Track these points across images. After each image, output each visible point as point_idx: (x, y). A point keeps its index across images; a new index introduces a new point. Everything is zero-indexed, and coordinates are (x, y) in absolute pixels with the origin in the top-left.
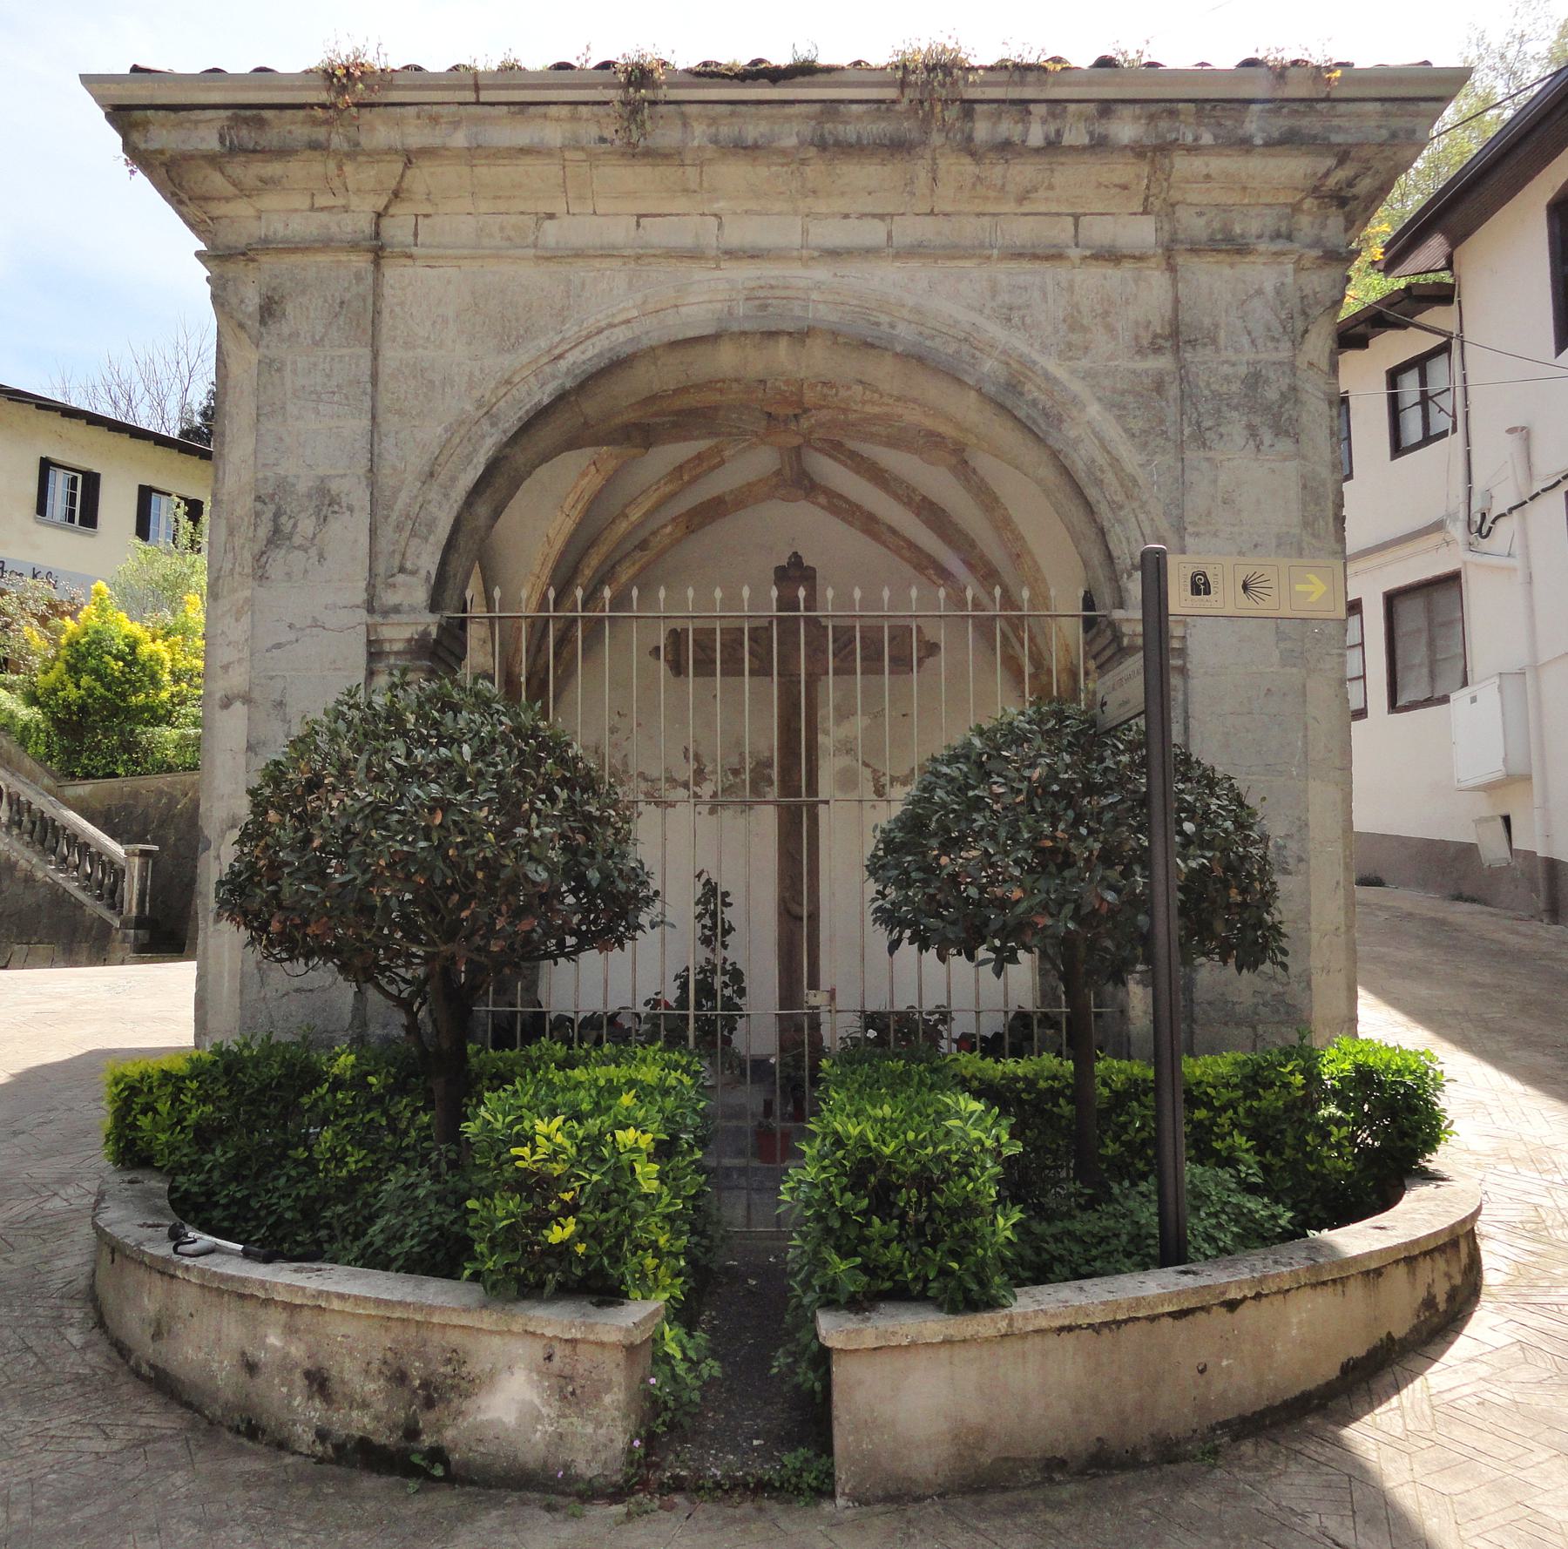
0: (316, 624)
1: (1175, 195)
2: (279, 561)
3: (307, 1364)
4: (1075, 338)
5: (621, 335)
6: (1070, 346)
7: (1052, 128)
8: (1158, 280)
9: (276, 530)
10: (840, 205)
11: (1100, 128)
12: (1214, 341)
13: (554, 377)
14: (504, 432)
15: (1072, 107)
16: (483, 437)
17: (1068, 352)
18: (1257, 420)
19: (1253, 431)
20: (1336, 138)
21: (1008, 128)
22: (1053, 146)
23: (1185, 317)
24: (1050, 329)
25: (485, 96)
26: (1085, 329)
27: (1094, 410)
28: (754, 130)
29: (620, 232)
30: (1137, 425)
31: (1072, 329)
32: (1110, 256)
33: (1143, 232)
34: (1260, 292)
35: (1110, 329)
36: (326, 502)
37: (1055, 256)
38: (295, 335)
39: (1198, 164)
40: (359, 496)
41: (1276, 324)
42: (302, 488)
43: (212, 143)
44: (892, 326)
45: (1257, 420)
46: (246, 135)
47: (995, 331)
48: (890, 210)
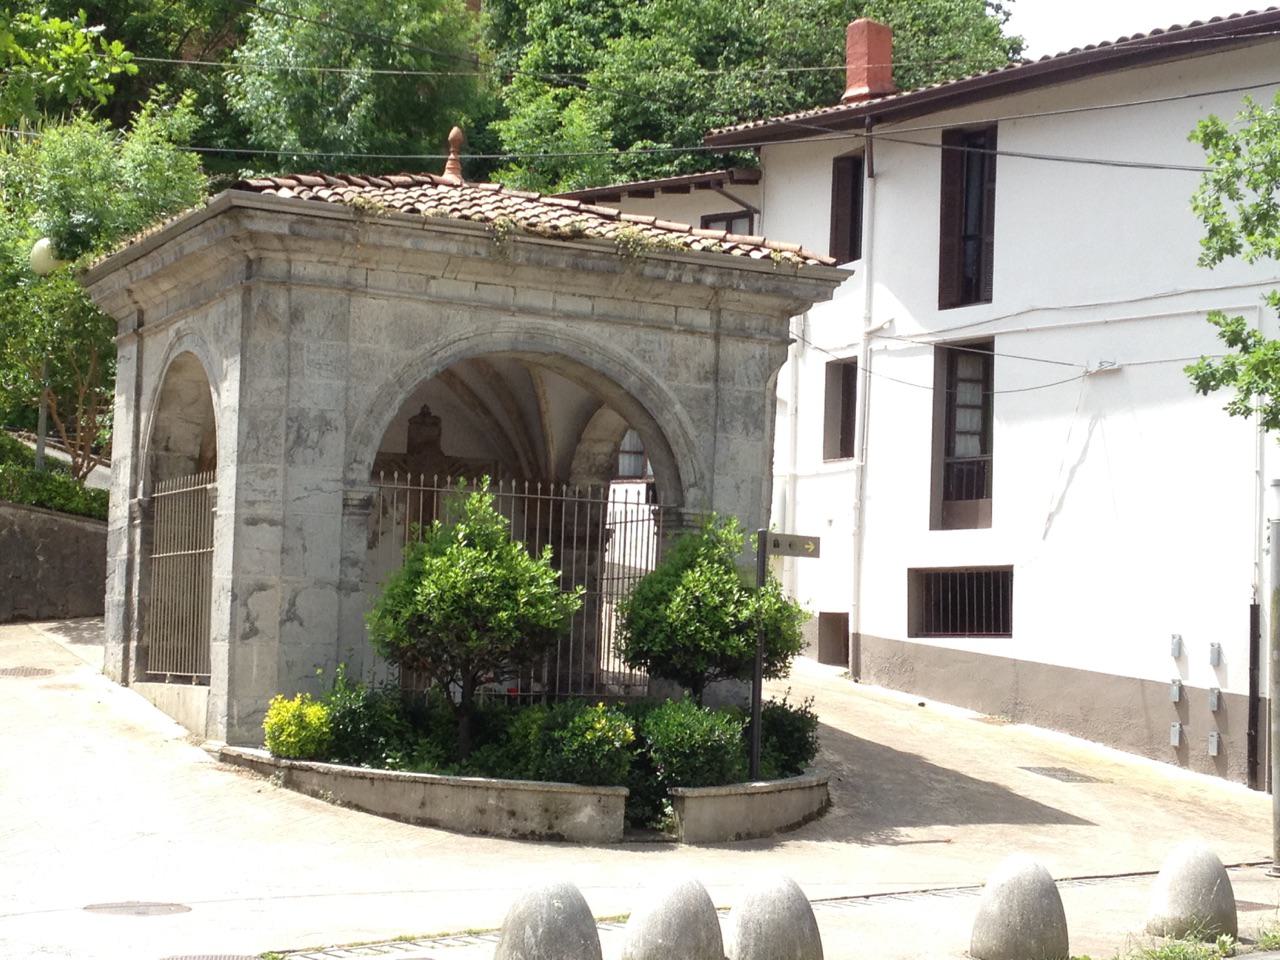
0: (319, 489)
1: (722, 306)
2: (300, 454)
3: (507, 808)
4: (673, 370)
5: (464, 344)
6: (670, 373)
7: (677, 273)
8: (709, 343)
9: (299, 437)
10: (572, 289)
11: (698, 276)
12: (733, 379)
13: (432, 364)
14: (408, 392)
15: (689, 266)
16: (396, 392)
17: (669, 376)
18: (748, 420)
19: (746, 427)
20: (796, 293)
21: (659, 271)
22: (678, 280)
23: (722, 366)
24: (661, 364)
25: (426, 227)
26: (677, 366)
27: (678, 407)
28: (546, 258)
29: (466, 291)
30: (697, 417)
31: (671, 365)
32: (690, 330)
33: (704, 319)
34: (753, 357)
35: (688, 367)
36: (325, 424)
37: (666, 328)
38: (309, 331)
39: (736, 295)
40: (341, 422)
41: (758, 373)
42: (312, 415)
43: (285, 230)
44: (591, 354)
45: (748, 420)
46: (304, 229)
47: (638, 363)
48: (594, 294)
